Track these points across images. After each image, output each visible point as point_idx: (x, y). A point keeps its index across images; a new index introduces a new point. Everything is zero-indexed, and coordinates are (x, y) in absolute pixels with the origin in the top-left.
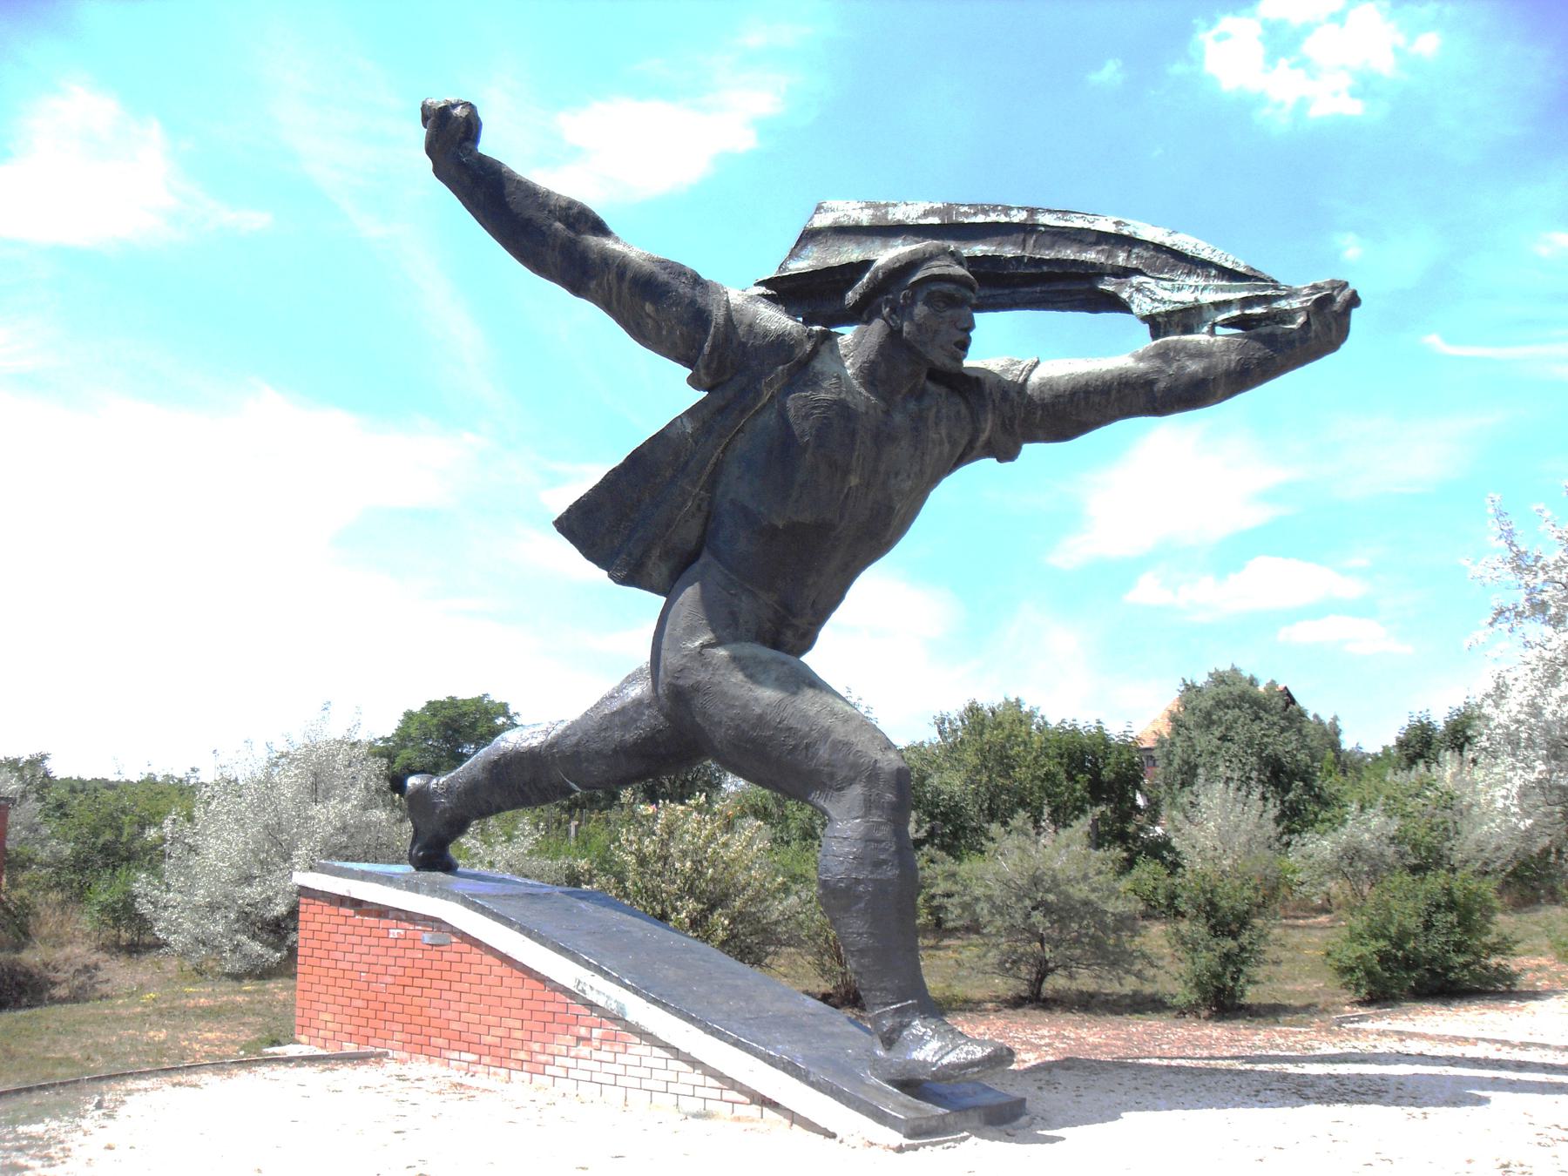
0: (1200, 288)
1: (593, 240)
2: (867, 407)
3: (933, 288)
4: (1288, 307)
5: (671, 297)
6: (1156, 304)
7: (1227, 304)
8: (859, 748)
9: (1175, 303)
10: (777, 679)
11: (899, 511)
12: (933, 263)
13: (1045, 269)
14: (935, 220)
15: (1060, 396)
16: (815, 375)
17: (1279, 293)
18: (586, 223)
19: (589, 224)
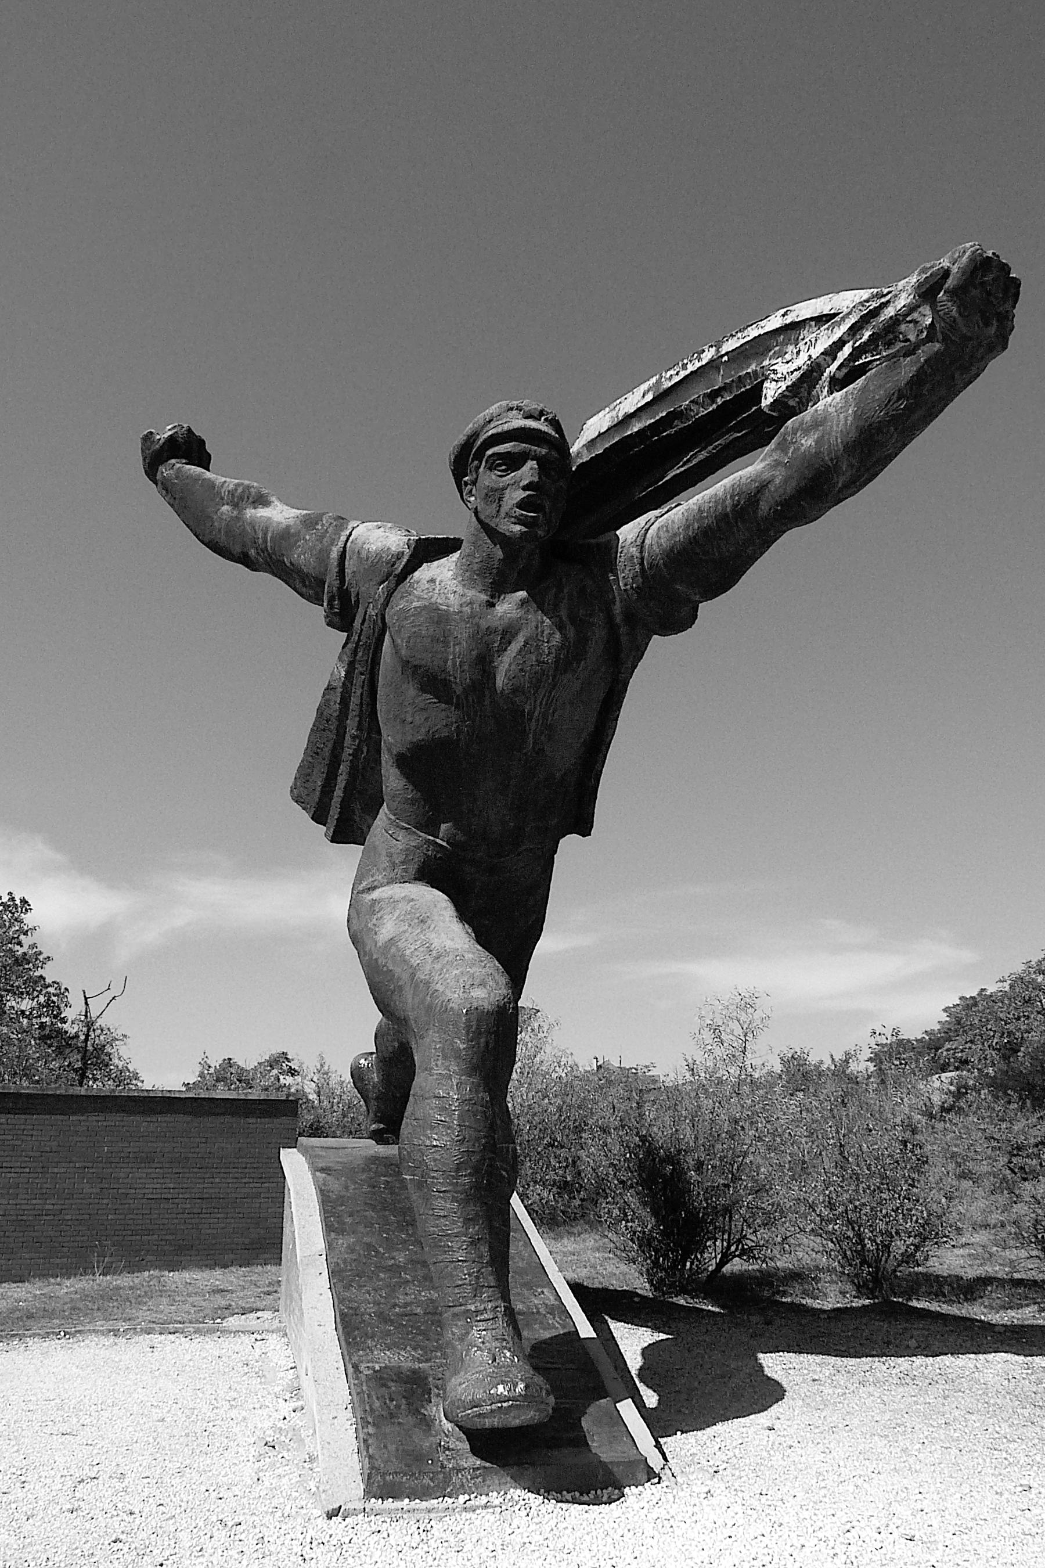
0: (813, 340)
1: (250, 513)
2: (461, 605)
3: (489, 452)
4: (892, 314)
5: (299, 546)
6: (780, 384)
7: (840, 344)
8: (438, 987)
9: (792, 373)
10: (397, 918)
11: (531, 713)
12: (492, 425)
13: (719, 401)
14: (649, 397)
15: (675, 535)
16: (411, 585)
17: (883, 300)
18: (248, 498)
19: (251, 499)
